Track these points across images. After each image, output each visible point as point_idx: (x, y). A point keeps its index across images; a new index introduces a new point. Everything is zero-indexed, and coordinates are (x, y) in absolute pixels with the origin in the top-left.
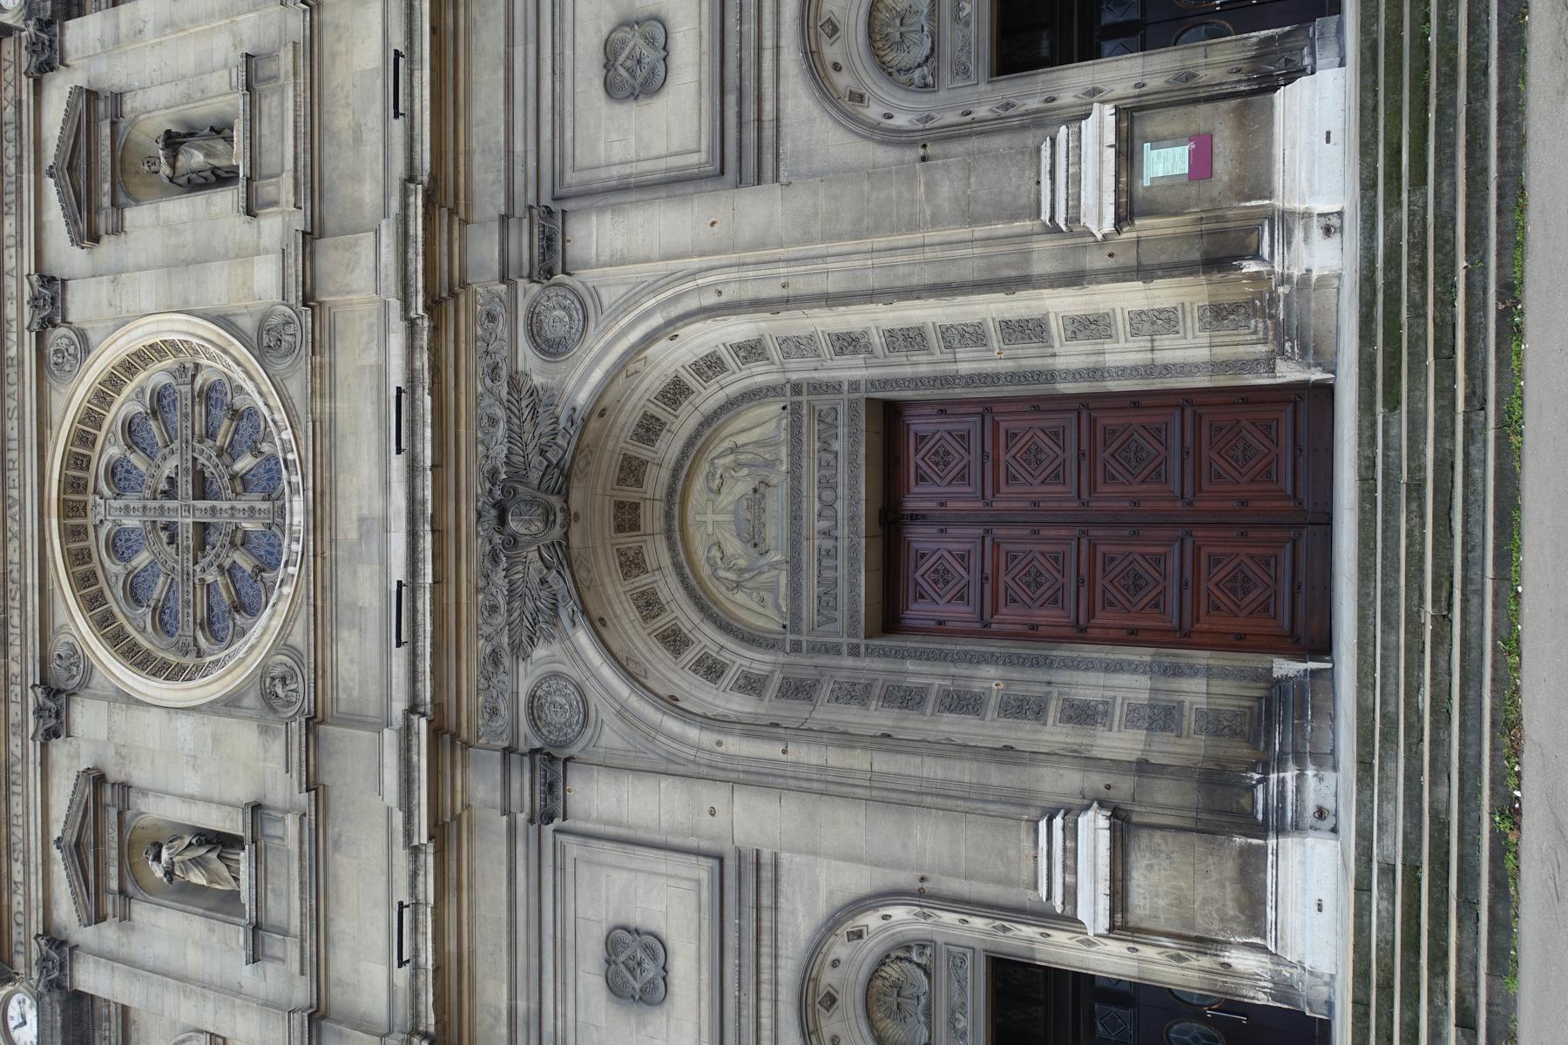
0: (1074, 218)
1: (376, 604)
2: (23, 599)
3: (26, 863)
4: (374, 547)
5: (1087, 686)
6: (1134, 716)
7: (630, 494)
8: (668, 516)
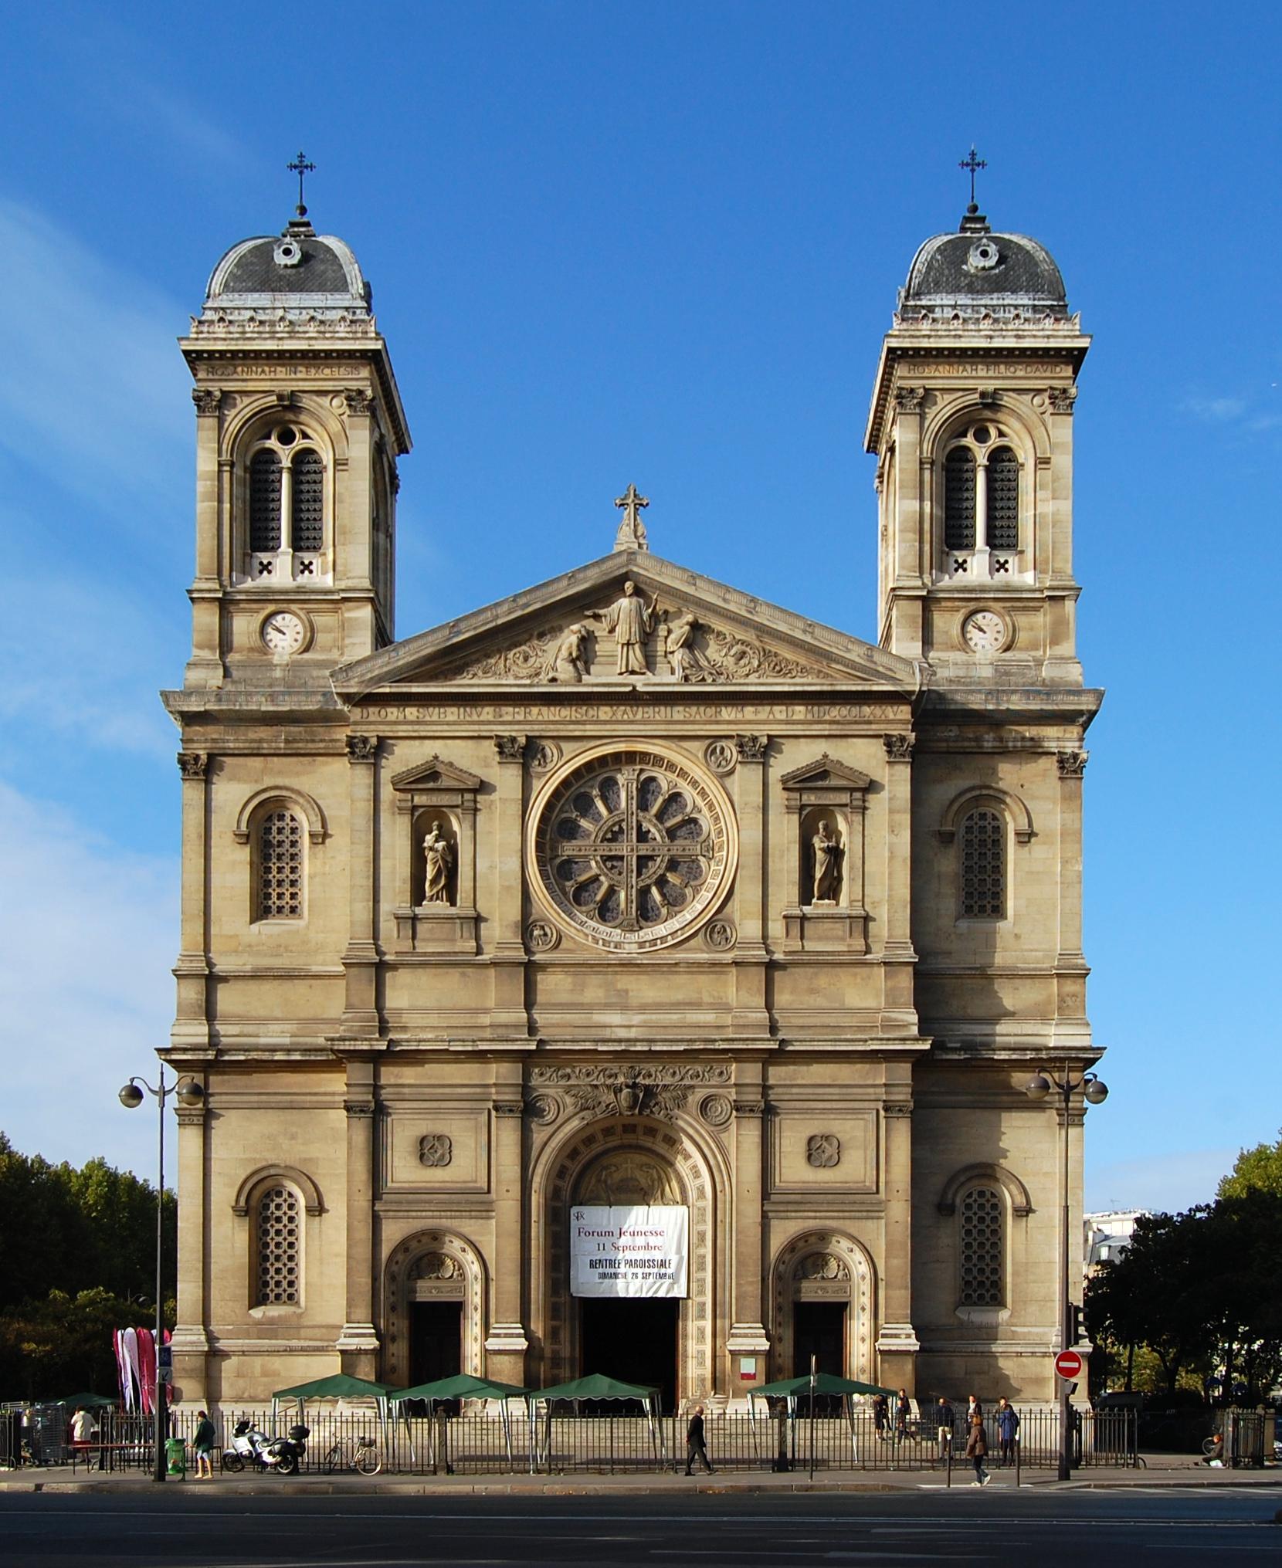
0: (733, 1336)
1: (586, 1001)
2: (577, 722)
3: (418, 723)
4: (614, 1000)
5: (565, 1335)
6: (555, 1353)
7: (640, 1130)
8: (630, 1146)
